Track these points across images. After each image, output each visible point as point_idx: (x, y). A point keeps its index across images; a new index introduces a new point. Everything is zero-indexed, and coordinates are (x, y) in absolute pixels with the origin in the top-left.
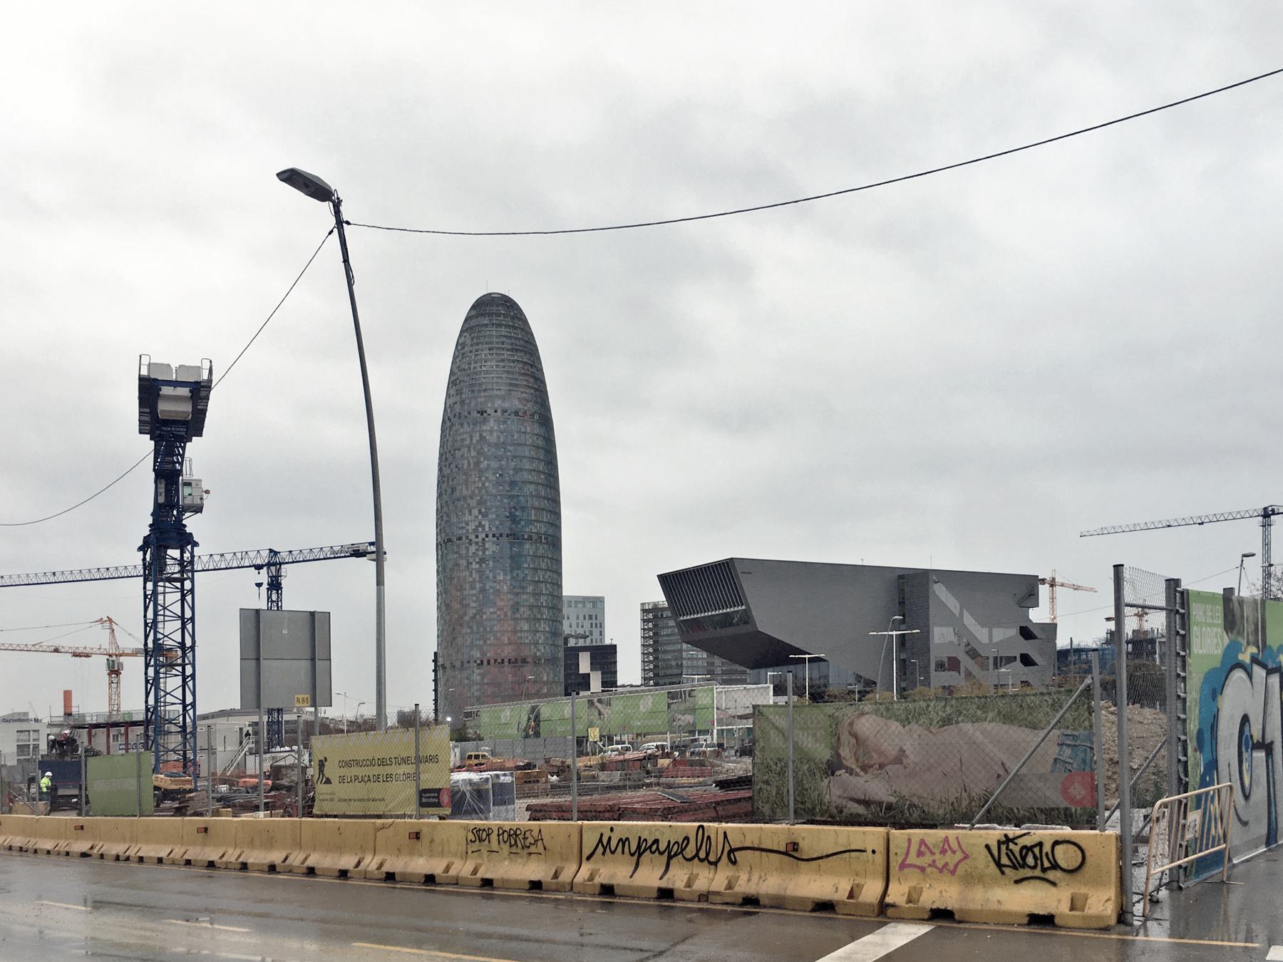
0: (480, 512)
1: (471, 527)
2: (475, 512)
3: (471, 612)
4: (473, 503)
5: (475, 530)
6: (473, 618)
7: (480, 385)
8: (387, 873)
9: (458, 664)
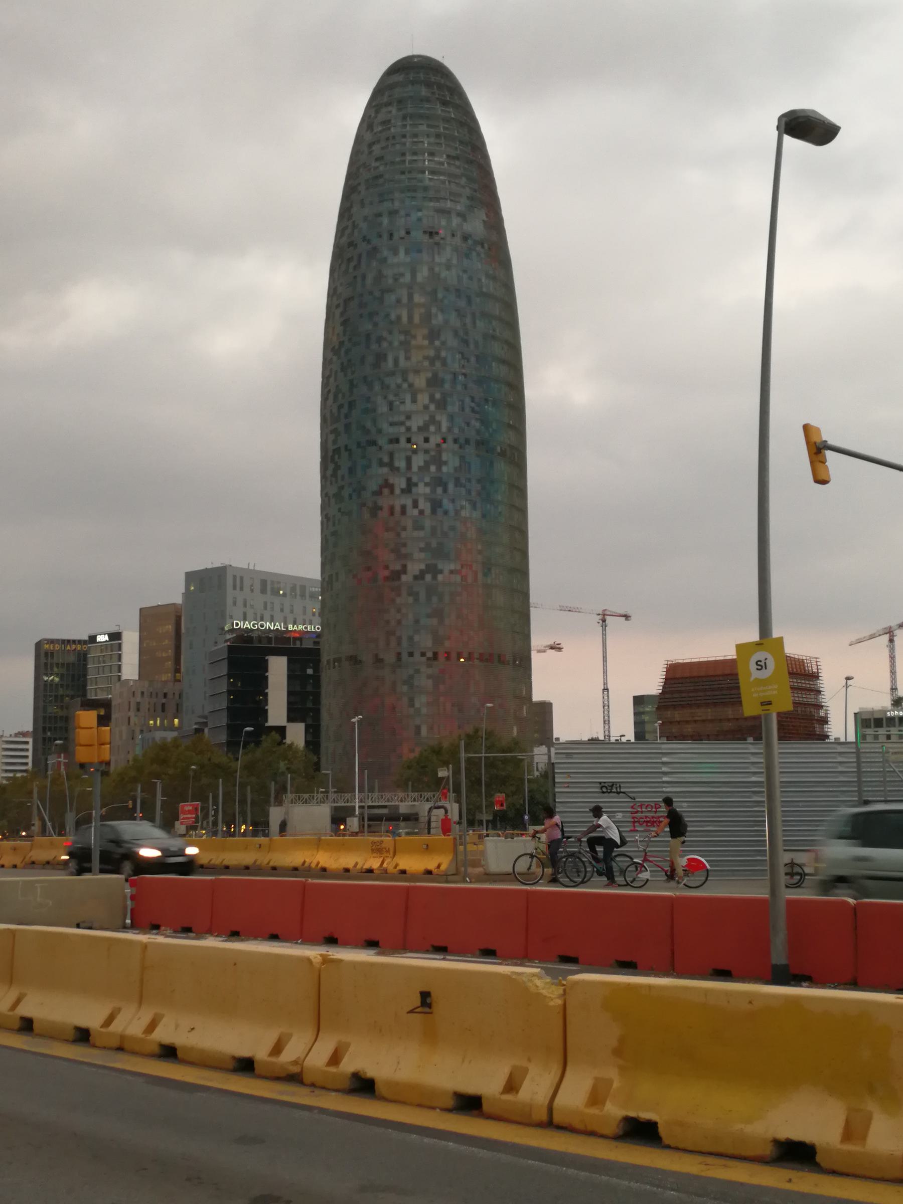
0: (432, 399)
1: (416, 423)
2: (423, 399)
3: (414, 568)
4: (420, 381)
5: (423, 429)
6: (420, 577)
7: (426, 189)
8: (356, 1076)
9: (390, 658)
